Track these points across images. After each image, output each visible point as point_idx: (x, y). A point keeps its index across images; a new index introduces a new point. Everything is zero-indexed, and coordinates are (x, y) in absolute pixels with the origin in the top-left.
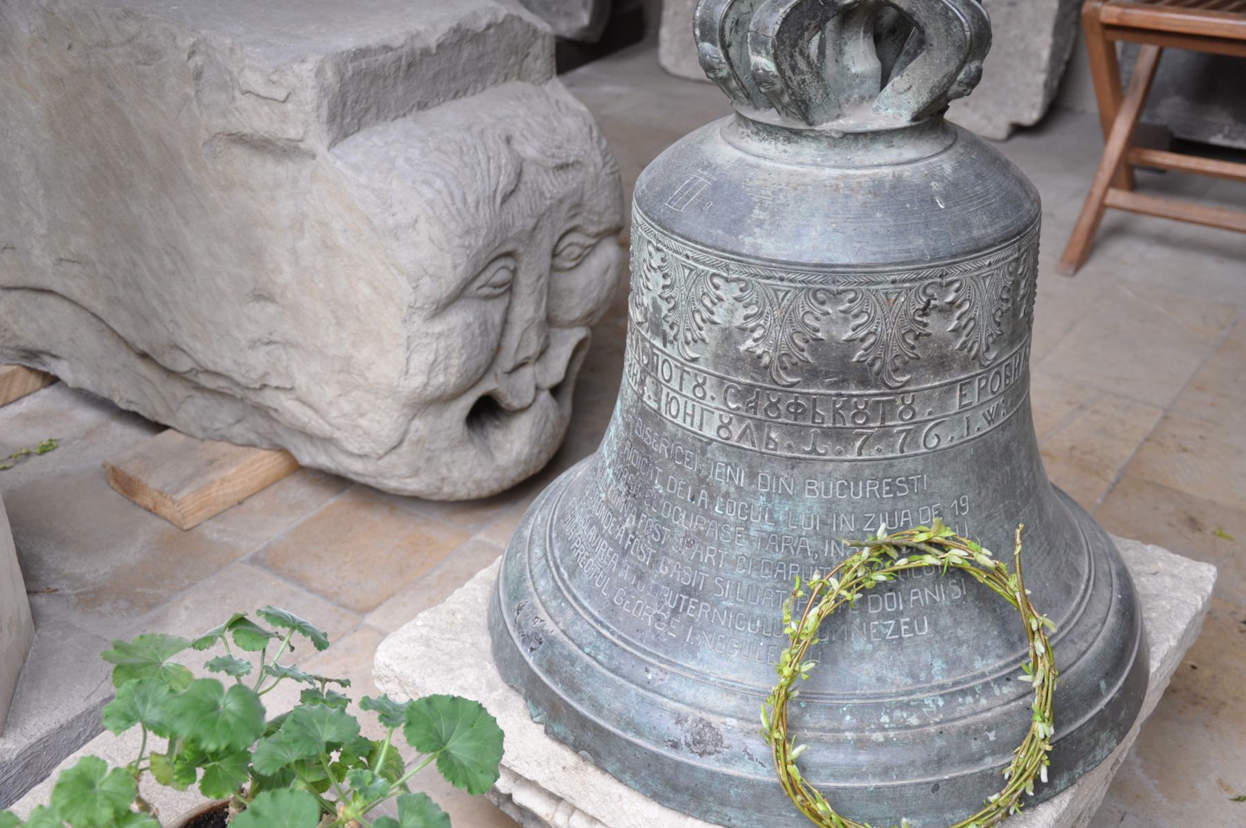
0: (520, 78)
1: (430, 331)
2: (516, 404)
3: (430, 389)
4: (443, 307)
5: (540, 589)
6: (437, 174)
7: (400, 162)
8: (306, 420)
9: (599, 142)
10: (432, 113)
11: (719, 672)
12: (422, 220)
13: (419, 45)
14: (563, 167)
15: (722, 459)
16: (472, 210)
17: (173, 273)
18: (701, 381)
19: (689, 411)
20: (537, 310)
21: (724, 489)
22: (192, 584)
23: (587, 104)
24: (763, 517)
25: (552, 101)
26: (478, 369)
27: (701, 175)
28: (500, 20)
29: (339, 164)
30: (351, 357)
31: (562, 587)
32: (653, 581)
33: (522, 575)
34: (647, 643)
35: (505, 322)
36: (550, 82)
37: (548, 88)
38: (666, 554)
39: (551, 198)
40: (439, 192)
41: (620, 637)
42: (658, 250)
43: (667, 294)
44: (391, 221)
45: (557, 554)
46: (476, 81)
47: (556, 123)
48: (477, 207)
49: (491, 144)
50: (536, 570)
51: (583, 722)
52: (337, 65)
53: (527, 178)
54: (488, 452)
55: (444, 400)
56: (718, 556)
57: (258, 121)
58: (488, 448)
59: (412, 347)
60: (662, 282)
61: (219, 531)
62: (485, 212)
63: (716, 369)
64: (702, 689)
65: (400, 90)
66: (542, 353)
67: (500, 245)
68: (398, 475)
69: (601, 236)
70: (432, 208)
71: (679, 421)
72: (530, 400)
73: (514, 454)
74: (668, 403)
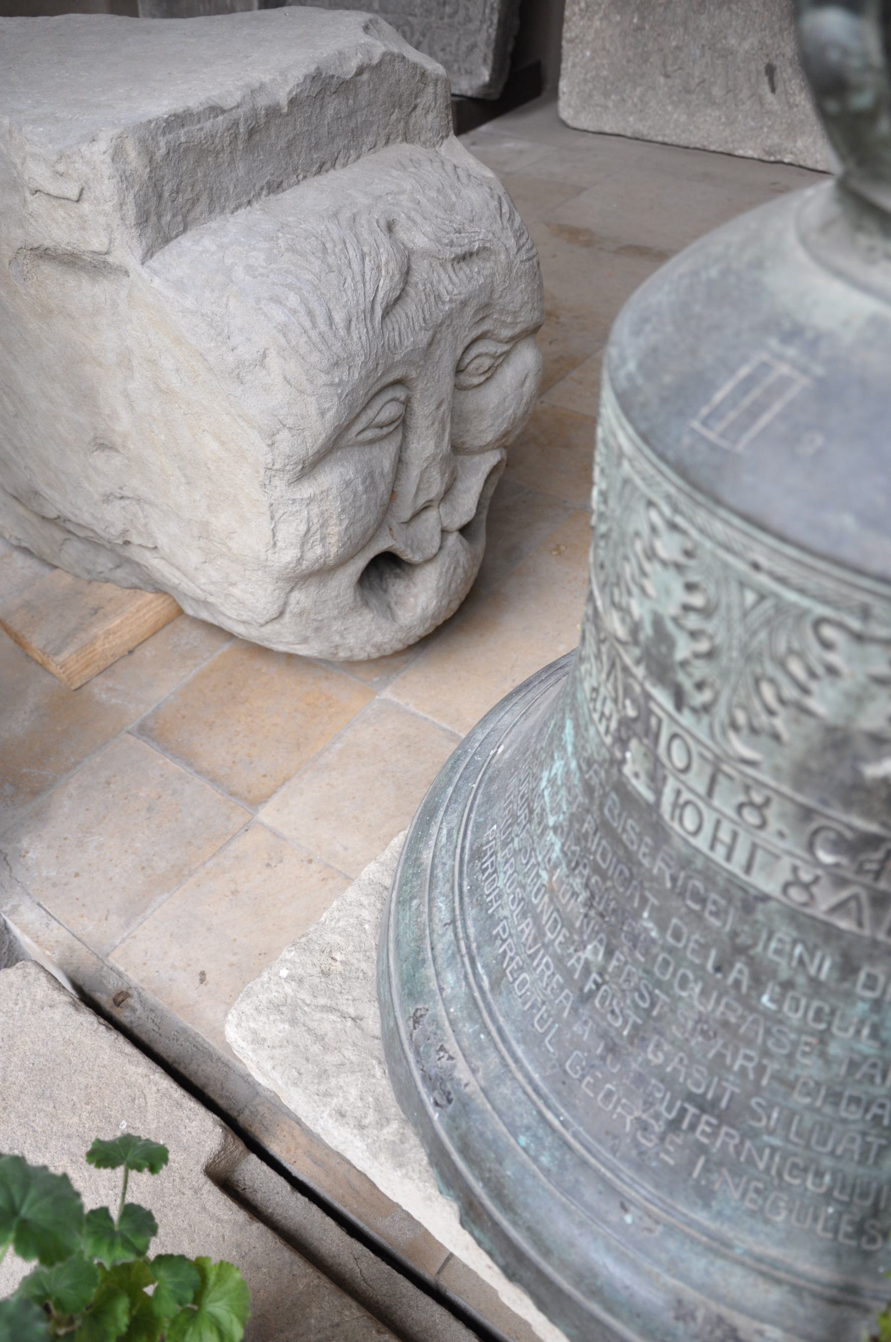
0: (406, 139)
1: (297, 496)
2: (417, 558)
3: (305, 564)
4: (309, 467)
5: (448, 991)
6: (289, 287)
7: (239, 273)
8: (177, 582)
9: (511, 219)
10: (287, 197)
11: (750, 1239)
12: (272, 355)
13: (263, 102)
14: (465, 257)
15: (785, 932)
16: (342, 333)
17: (16, 416)
18: (758, 798)
19: (725, 835)
20: (437, 445)
21: (784, 974)
22: (78, 763)
23: (493, 169)
24: (858, 1032)
25: (449, 168)
26: (365, 532)
27: (780, 357)
28: (375, 61)
29: (157, 282)
30: (208, 523)
31: (481, 1004)
32: (634, 1066)
33: (419, 950)
34: (623, 1159)
35: (400, 462)
36: (445, 142)
37: (443, 150)
38: (661, 1033)
39: (451, 301)
40: (294, 312)
41: (575, 1135)
42: (673, 527)
43: (693, 621)
44: (230, 358)
45: (472, 931)
46: (347, 148)
47: (454, 198)
48: (348, 328)
49: (365, 234)
50: (439, 947)
51: (519, 1255)
52: (142, 141)
53: (416, 277)
54: (388, 612)
55: (323, 572)
56: (760, 1070)
57: (58, 232)
58: (389, 607)
59: (277, 516)
60: (680, 595)
61: (109, 689)
62: (359, 332)
63: (798, 786)
64: (720, 1263)
65: (241, 169)
66: (448, 492)
67: (383, 375)
68: (284, 638)
69: (515, 340)
70: (285, 335)
71: (701, 842)
72: (434, 551)
73: (419, 610)
74: (679, 807)
